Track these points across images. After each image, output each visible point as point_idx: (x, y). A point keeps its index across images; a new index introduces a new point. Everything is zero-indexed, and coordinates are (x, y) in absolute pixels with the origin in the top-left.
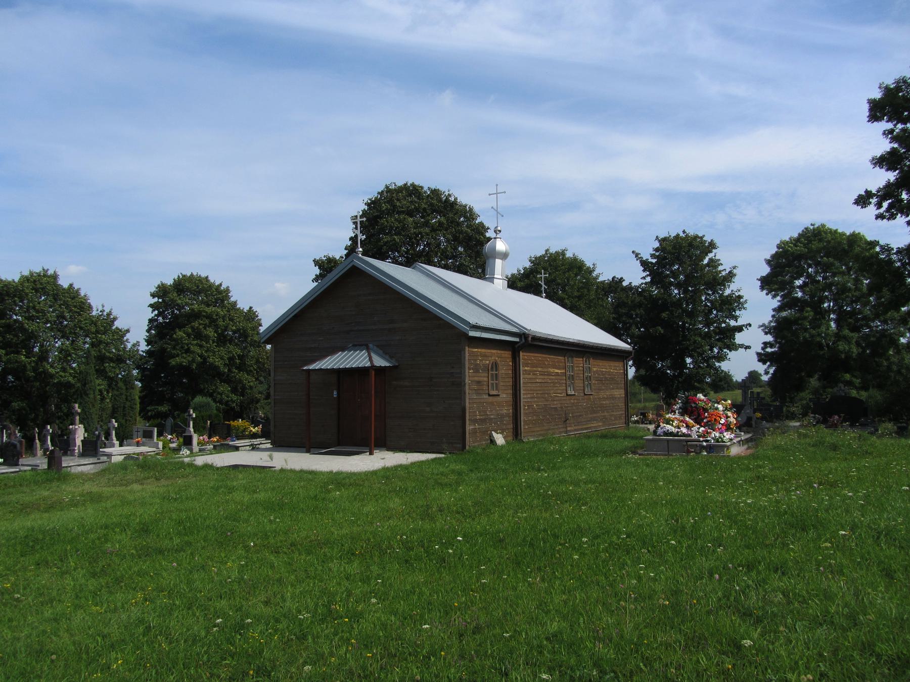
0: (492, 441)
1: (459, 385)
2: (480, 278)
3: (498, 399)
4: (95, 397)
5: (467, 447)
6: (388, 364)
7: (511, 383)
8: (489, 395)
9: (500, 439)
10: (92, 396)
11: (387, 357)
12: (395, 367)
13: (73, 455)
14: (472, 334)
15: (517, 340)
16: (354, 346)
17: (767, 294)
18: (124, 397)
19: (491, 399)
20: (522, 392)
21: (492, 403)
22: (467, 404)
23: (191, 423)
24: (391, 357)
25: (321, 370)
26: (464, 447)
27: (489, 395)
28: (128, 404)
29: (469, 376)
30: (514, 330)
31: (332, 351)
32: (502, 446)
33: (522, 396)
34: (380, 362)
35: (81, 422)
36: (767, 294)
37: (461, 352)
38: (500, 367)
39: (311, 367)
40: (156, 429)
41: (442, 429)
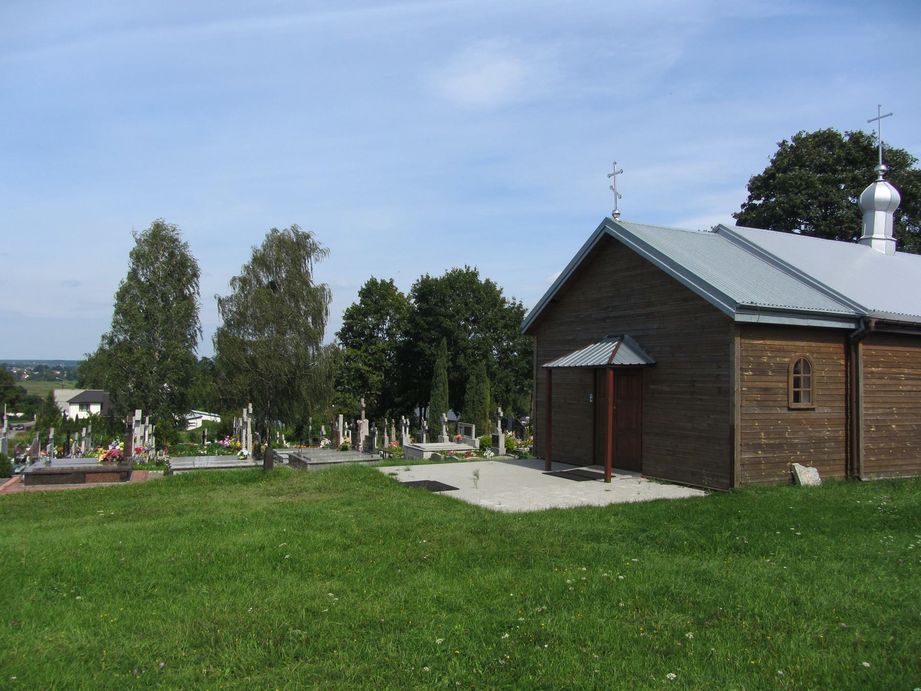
0: (794, 479)
1: (726, 393)
2: (845, 237)
3: (811, 414)
4: (444, 390)
5: (737, 485)
6: (642, 362)
7: (843, 392)
8: (789, 409)
9: (808, 476)
10: (441, 389)
11: (644, 353)
12: (647, 365)
13: (358, 450)
14: (739, 318)
15: (852, 326)
16: (610, 337)
17: (286, 256)
18: (474, 390)
19: (794, 415)
20: (862, 405)
21: (798, 422)
22: (737, 421)
23: (499, 422)
24: (648, 352)
25: (558, 367)
26: (732, 484)
27: (789, 409)
28: (477, 397)
29: (742, 381)
30: (851, 312)
31: (581, 344)
32: (812, 488)
33: (862, 411)
34: (627, 357)
35: (366, 418)
36: (286, 256)
37: (729, 344)
38: (816, 367)
39: (550, 365)
40: (474, 426)
41: (703, 455)
